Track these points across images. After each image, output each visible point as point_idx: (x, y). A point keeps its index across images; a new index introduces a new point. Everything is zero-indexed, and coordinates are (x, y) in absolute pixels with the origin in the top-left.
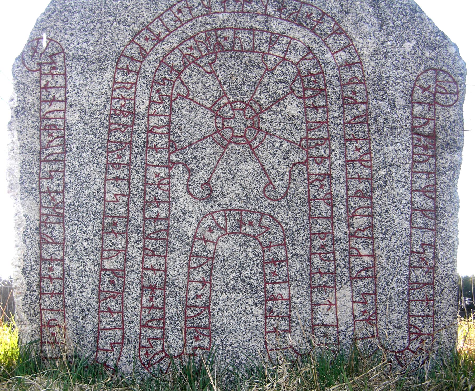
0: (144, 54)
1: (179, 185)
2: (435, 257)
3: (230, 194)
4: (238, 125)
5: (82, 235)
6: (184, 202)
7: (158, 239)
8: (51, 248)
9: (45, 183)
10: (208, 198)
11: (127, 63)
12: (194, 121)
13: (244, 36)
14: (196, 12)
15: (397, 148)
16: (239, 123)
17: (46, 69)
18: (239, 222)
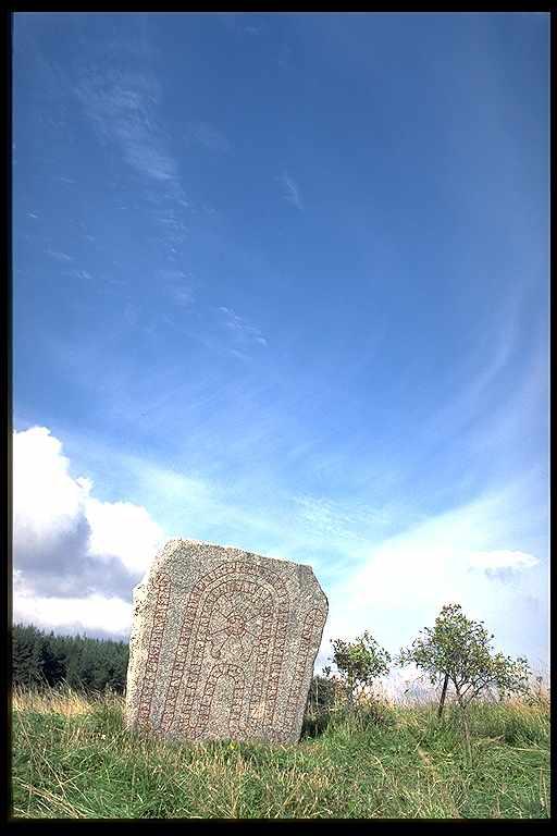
0: (205, 587)
1: (207, 650)
2: (300, 693)
3: (228, 657)
4: (236, 629)
5: (165, 669)
6: (209, 659)
7: (195, 675)
8: (150, 674)
9: (153, 643)
10: (218, 658)
11: (196, 590)
12: (219, 622)
13: (246, 585)
14: (230, 571)
15: (295, 644)
16: (236, 626)
17: (162, 588)
18: (230, 670)
